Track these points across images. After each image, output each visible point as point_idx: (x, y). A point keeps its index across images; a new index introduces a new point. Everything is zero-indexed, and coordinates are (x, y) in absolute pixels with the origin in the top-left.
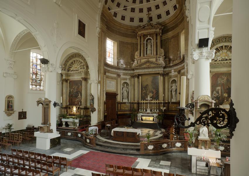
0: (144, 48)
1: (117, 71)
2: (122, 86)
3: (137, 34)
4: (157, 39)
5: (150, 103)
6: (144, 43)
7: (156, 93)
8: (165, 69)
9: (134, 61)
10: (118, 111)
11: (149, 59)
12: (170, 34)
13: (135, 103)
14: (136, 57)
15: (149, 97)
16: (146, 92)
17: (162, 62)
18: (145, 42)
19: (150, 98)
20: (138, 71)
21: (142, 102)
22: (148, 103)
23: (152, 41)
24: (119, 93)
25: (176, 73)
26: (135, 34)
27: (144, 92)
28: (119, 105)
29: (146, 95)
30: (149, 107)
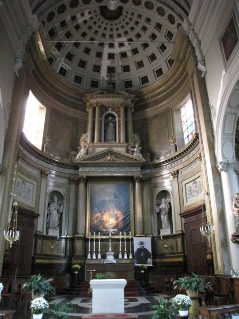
2: (48, 198)
3: (88, 104)
4: (126, 117)
5: (113, 240)
8: (143, 171)
9: (77, 151)
10: (36, 256)
13: (80, 238)
14: (82, 144)
18: (103, 119)
20: (87, 169)
21: (95, 237)
22: (109, 239)
23: (117, 119)
24: (41, 212)
26: (81, 103)
27: (97, 215)
28: (39, 242)
30: (110, 249)
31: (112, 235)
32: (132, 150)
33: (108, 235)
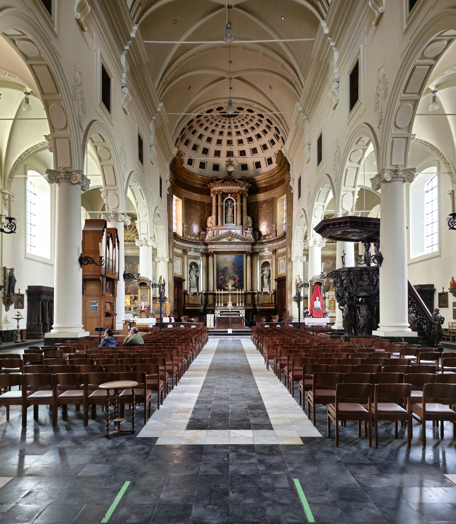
0: (222, 212)
1: (183, 244)
4: (242, 201)
5: (232, 294)
6: (222, 206)
7: (239, 280)
11: (231, 231)
12: (262, 197)
14: (209, 225)
15: (230, 286)
16: (225, 277)
17: (250, 237)
18: (224, 204)
19: (232, 287)
20: (214, 246)
21: (219, 292)
22: (228, 294)
23: (235, 204)
24: (186, 277)
25: (271, 253)
27: (221, 277)
29: (225, 282)
30: (230, 300)
31: (231, 291)
32: (246, 231)
33: (229, 290)
